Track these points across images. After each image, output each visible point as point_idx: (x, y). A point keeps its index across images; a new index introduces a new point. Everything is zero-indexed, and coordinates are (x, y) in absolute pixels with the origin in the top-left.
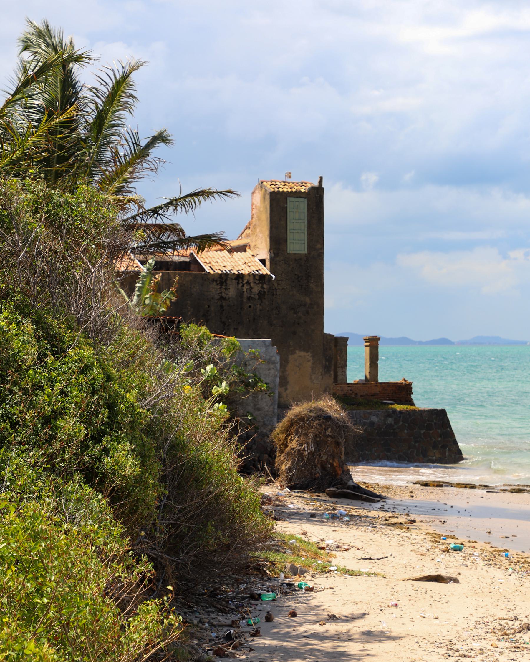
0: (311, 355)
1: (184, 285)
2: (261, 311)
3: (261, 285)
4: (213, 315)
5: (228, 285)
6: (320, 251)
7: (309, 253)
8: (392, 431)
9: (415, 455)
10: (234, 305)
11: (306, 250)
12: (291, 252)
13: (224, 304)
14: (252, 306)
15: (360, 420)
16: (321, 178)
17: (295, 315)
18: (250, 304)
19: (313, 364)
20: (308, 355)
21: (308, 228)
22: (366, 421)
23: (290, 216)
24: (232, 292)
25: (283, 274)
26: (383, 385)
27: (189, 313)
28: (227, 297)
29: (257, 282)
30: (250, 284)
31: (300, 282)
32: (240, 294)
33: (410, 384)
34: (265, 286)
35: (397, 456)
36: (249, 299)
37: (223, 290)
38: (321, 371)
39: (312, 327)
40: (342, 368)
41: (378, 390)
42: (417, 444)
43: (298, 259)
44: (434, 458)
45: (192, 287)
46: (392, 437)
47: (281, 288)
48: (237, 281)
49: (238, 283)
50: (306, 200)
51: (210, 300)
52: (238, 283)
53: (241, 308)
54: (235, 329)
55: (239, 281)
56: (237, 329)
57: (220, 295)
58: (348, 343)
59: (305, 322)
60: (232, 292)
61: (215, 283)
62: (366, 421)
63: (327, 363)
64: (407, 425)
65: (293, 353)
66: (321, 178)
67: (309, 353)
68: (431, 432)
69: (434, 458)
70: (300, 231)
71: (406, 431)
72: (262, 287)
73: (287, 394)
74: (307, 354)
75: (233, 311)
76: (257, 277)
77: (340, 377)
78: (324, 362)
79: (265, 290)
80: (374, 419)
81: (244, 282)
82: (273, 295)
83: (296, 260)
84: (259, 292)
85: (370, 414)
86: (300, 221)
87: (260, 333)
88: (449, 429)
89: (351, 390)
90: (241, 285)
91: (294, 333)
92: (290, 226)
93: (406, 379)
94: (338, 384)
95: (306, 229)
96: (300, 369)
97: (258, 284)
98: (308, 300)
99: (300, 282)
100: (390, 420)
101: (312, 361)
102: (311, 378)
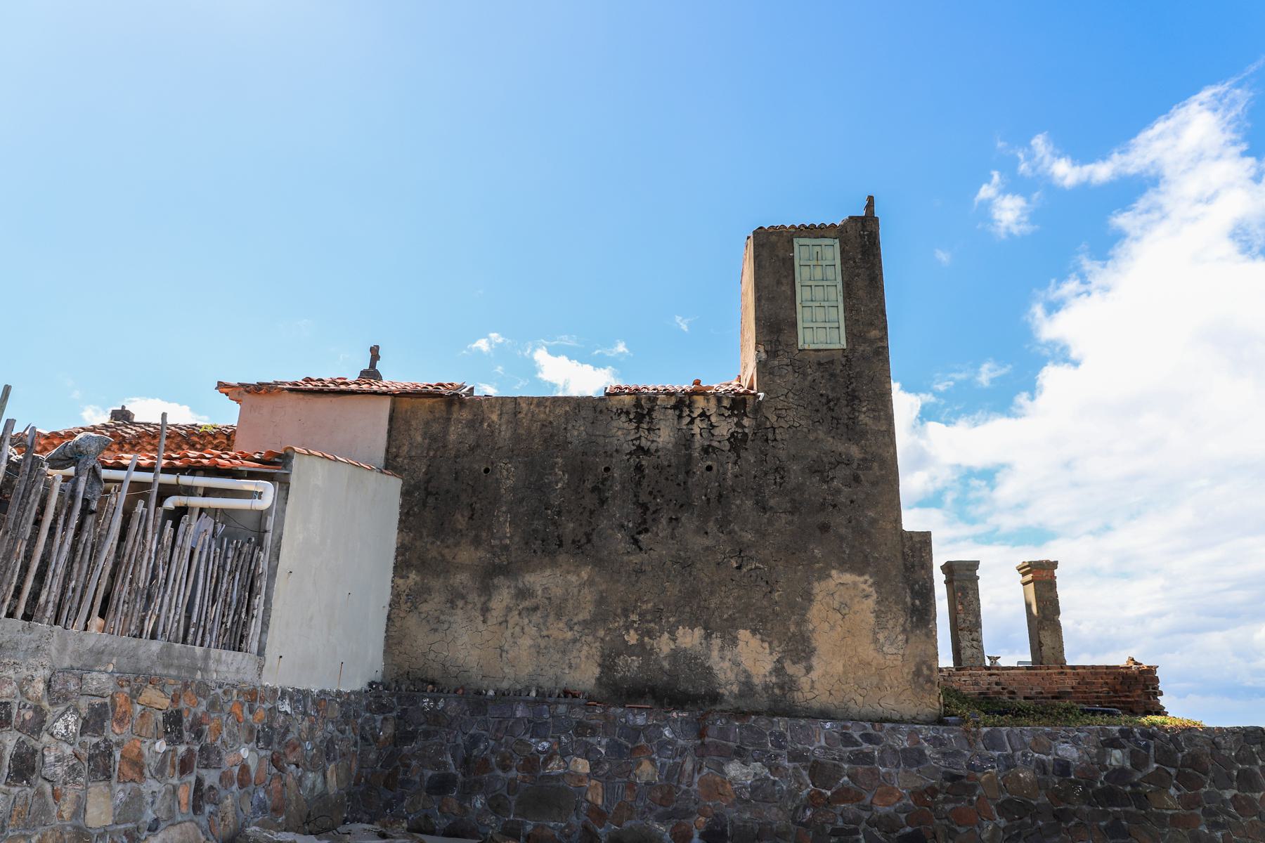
0: (871, 581)
1: (551, 423)
2: (736, 476)
3: (735, 420)
4: (617, 488)
5: (655, 421)
6: (880, 344)
7: (853, 350)
8: (1128, 789)
10: (669, 466)
11: (844, 342)
12: (806, 347)
13: (643, 463)
14: (715, 468)
15: (1024, 755)
16: (871, 199)
17: (825, 487)
18: (709, 463)
20: (866, 582)
21: (844, 298)
22: (1044, 757)
23: (801, 274)
24: (665, 435)
25: (791, 395)
27: (560, 485)
28: (653, 447)
29: (727, 413)
30: (709, 417)
31: (833, 410)
32: (686, 441)
34: (746, 422)
36: (706, 450)
37: (643, 433)
38: (901, 620)
43: (825, 362)
45: (570, 427)
46: (1133, 809)
47: (786, 426)
48: (677, 412)
49: (680, 417)
50: (837, 241)
51: (611, 456)
52: (680, 417)
53: (687, 473)
54: (671, 519)
55: (681, 411)
56: (676, 519)
57: (637, 443)
59: (852, 502)
60: (665, 435)
61: (623, 418)
62: (1044, 757)
63: (917, 602)
64: (1173, 771)
65: (824, 575)
66: (871, 199)
67: (867, 577)
70: (826, 304)
71: (1172, 791)
72: (739, 424)
73: (813, 682)
74: (862, 579)
75: (667, 479)
76: (726, 403)
78: (908, 599)
79: (746, 430)
80: (1068, 751)
81: (695, 415)
82: (767, 440)
83: (820, 364)
84: (732, 434)
85: (1053, 737)
86: (825, 283)
87: (736, 528)
90: (688, 419)
91: (825, 528)
92: (802, 294)
95: (841, 299)
96: (844, 616)
97: (729, 416)
98: (855, 451)
99: (833, 410)
100: (1117, 757)
101: (875, 596)
102: (876, 641)
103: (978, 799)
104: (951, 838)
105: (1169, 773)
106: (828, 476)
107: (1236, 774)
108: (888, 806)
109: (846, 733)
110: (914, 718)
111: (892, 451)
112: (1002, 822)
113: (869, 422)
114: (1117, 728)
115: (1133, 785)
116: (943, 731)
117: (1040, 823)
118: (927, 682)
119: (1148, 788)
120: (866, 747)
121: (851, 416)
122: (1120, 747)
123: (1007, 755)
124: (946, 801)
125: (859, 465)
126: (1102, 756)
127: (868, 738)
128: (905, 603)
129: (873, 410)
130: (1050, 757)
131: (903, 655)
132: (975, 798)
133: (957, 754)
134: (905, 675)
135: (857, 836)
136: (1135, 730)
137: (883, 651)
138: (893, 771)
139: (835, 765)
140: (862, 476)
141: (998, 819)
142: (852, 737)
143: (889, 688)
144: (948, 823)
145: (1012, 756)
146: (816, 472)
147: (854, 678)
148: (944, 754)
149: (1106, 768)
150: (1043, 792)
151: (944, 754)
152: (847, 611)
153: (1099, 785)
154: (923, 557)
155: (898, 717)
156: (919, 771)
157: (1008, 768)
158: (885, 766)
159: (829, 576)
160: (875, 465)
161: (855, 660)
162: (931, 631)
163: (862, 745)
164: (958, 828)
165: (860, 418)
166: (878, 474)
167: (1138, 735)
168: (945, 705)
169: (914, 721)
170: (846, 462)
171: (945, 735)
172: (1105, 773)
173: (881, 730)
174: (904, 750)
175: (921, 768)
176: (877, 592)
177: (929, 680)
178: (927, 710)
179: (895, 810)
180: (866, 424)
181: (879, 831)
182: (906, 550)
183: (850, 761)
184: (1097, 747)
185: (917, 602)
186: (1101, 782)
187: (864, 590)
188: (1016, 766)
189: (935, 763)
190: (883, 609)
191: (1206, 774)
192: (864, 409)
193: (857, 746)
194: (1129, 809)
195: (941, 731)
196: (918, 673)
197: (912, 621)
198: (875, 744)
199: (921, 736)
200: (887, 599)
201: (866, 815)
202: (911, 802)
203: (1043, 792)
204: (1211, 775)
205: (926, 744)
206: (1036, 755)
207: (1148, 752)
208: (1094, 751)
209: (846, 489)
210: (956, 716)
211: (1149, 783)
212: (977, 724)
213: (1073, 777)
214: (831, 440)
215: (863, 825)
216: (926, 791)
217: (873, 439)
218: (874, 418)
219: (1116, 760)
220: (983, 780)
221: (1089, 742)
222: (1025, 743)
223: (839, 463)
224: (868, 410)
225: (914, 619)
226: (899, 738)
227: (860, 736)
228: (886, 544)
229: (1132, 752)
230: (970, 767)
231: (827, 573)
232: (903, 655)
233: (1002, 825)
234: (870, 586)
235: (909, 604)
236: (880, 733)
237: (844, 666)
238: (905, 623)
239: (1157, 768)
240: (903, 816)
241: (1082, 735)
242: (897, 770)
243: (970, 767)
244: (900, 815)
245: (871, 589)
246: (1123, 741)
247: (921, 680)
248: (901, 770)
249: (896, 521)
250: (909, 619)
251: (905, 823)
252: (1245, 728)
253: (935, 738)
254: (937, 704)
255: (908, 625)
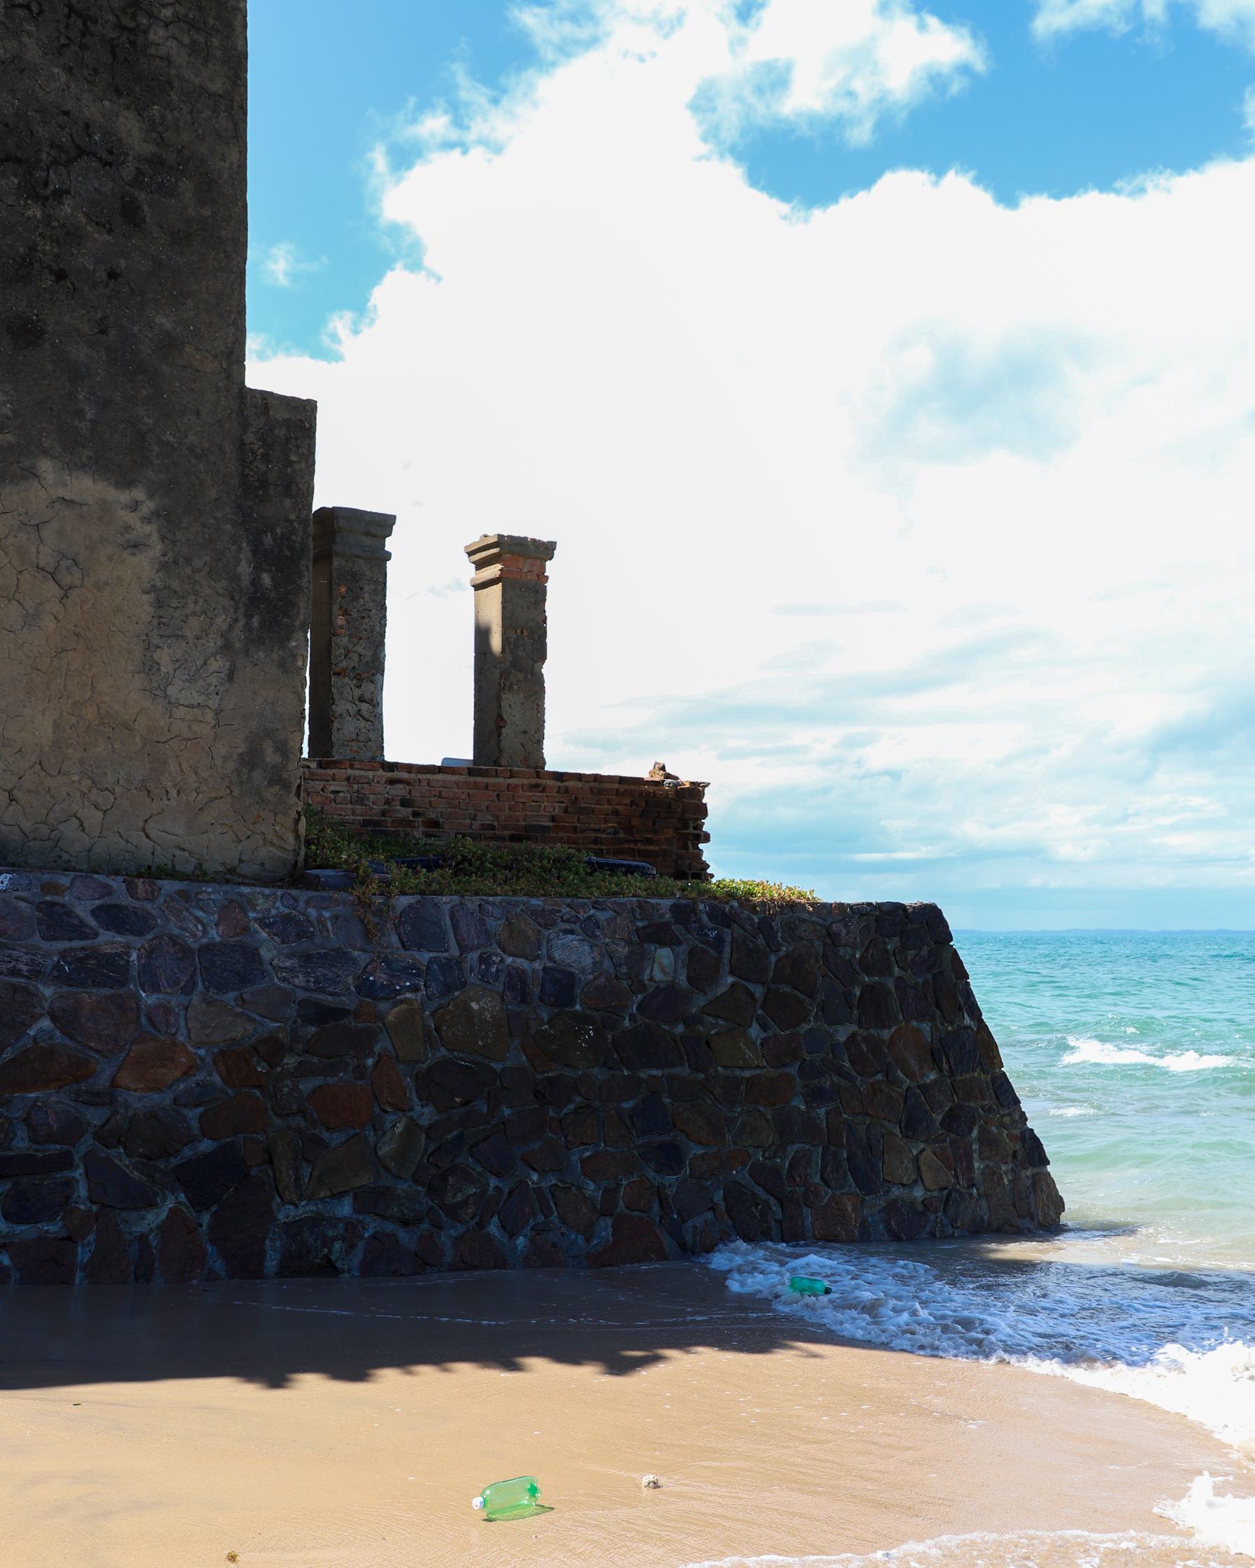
0: (148, 506)
8: (680, 1029)
9: (817, 1179)
17: (35, 211)
19: (164, 567)
20: (134, 506)
22: (523, 963)
26: (570, 784)
33: (697, 790)
35: (718, 1196)
38: (221, 622)
39: (165, 321)
40: (359, 679)
41: (550, 806)
42: (822, 1111)
44: (919, 1193)
46: (684, 1071)
58: (390, 544)
59: (112, 275)
62: (523, 963)
63: (266, 579)
64: (758, 991)
67: (138, 494)
68: (886, 1034)
69: (919, 1193)
71: (755, 1031)
74: (124, 497)
77: (345, 729)
78: (245, 569)
85: (545, 920)
88: (967, 1020)
89: (405, 803)
93: (668, 770)
94: (336, 764)
96: (66, 591)
101: (158, 548)
102: (150, 667)
103: (376, 1064)
104: (306, 1160)
105: (752, 995)
106: (46, 184)
107: (858, 993)
108: (160, 1090)
109: (56, 904)
110: (232, 871)
111: (234, 157)
112: (426, 1115)
113: (181, 58)
114: (668, 902)
115: (690, 1021)
116: (308, 903)
117: (507, 1112)
118: (271, 783)
119: (713, 1026)
120: (108, 941)
121: (126, 21)
122: (673, 942)
123: (449, 960)
124: (303, 1070)
125: (140, 172)
126: (638, 959)
127: (113, 917)
128: (236, 578)
129: (193, 25)
130: (537, 965)
131: (218, 712)
132: (370, 1062)
133: (339, 957)
134: (219, 762)
135: (67, 1174)
136: (701, 907)
137: (166, 696)
138: (176, 1001)
139: (15, 989)
140: (146, 208)
141: (418, 1108)
142: (69, 913)
143: (173, 793)
144: (303, 1124)
145: (459, 963)
146: (18, 161)
147: (81, 762)
148: (307, 958)
149: (642, 987)
150: (517, 1042)
151: (307, 959)
152: (75, 577)
153: (627, 1023)
154: (290, 463)
155: (189, 868)
156: (242, 1001)
157: (448, 989)
158: (155, 988)
159: (32, 473)
160: (187, 187)
161: (90, 713)
162: (294, 656)
163: (96, 934)
164: (326, 1135)
165: (151, 36)
166: (191, 212)
167: (705, 918)
168: (308, 843)
169: (230, 876)
170: (105, 155)
171: (312, 912)
172: (640, 997)
173: (151, 898)
174: (208, 949)
175: (247, 992)
176: (163, 538)
177: (277, 778)
178: (264, 852)
179: (175, 1101)
180: (168, 60)
181: (129, 1156)
182: (250, 437)
183: (59, 977)
184: (629, 942)
185: (266, 579)
186: (632, 1018)
187: (128, 528)
188: (464, 984)
189: (284, 979)
190: (175, 584)
191: (811, 996)
192: (167, 13)
193: (84, 936)
194: (677, 1071)
195: (302, 904)
196: (251, 759)
197: (248, 626)
198: (133, 933)
199: (252, 915)
200: (188, 561)
201: (94, 1117)
202: (216, 1078)
203: (517, 1042)
204: (821, 996)
205: (264, 935)
206: (509, 960)
207: (720, 952)
208: (623, 950)
209: (98, 237)
210: (334, 867)
211: (717, 1017)
212: (386, 889)
213: (578, 1007)
214: (64, 78)
215: (87, 1143)
216: (255, 1048)
217: (186, 109)
218: (193, 48)
219: (662, 970)
220: (391, 1018)
221: (614, 932)
222: (487, 932)
223: (81, 152)
224: (177, 18)
225: (255, 621)
226: (198, 920)
227: (93, 912)
228: (198, 413)
229: (691, 953)
230: (366, 988)
231: (27, 463)
232: (218, 712)
233: (425, 1122)
234: (147, 520)
235: (245, 582)
236: (148, 906)
237: (56, 726)
238: (231, 628)
239: (733, 985)
240: (192, 1115)
241: (602, 916)
242: (184, 999)
243: (366, 988)
244: (186, 1111)
245: (148, 529)
246: (677, 929)
247: (258, 776)
248: (196, 998)
249: (231, 353)
250: (242, 621)
251: (196, 1131)
252: (879, 906)
253: (287, 919)
254: (291, 838)
255: (238, 635)
